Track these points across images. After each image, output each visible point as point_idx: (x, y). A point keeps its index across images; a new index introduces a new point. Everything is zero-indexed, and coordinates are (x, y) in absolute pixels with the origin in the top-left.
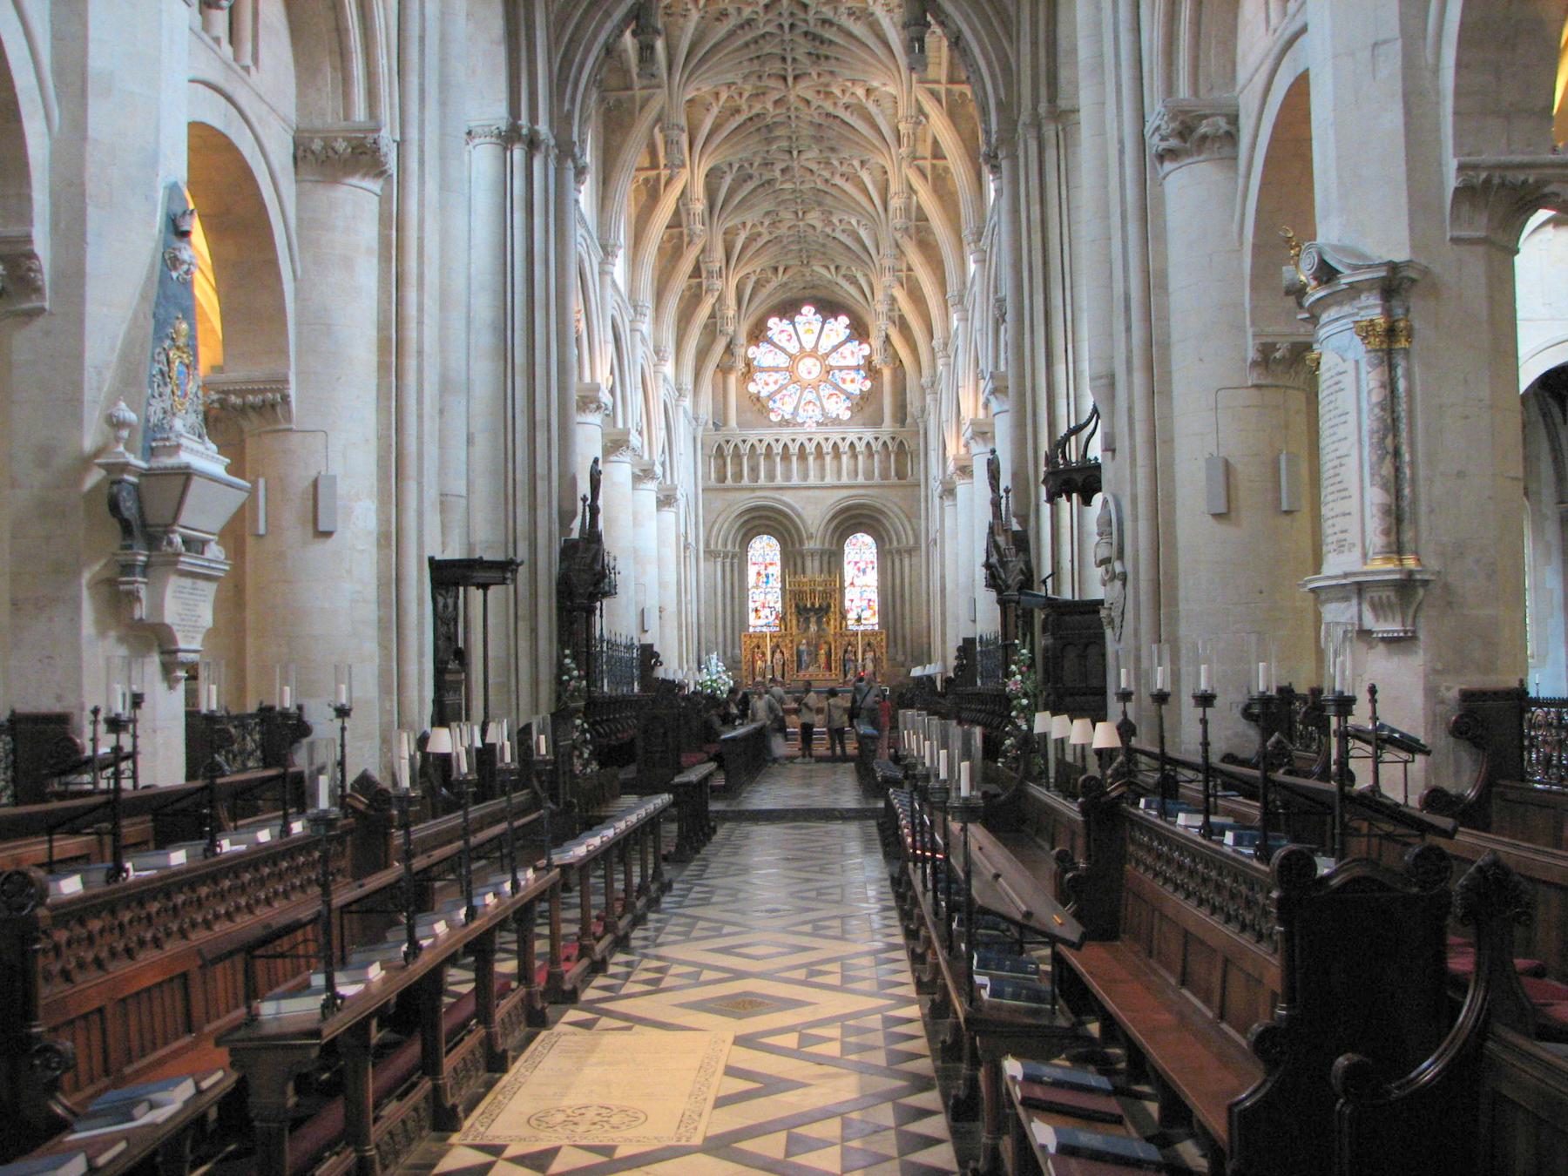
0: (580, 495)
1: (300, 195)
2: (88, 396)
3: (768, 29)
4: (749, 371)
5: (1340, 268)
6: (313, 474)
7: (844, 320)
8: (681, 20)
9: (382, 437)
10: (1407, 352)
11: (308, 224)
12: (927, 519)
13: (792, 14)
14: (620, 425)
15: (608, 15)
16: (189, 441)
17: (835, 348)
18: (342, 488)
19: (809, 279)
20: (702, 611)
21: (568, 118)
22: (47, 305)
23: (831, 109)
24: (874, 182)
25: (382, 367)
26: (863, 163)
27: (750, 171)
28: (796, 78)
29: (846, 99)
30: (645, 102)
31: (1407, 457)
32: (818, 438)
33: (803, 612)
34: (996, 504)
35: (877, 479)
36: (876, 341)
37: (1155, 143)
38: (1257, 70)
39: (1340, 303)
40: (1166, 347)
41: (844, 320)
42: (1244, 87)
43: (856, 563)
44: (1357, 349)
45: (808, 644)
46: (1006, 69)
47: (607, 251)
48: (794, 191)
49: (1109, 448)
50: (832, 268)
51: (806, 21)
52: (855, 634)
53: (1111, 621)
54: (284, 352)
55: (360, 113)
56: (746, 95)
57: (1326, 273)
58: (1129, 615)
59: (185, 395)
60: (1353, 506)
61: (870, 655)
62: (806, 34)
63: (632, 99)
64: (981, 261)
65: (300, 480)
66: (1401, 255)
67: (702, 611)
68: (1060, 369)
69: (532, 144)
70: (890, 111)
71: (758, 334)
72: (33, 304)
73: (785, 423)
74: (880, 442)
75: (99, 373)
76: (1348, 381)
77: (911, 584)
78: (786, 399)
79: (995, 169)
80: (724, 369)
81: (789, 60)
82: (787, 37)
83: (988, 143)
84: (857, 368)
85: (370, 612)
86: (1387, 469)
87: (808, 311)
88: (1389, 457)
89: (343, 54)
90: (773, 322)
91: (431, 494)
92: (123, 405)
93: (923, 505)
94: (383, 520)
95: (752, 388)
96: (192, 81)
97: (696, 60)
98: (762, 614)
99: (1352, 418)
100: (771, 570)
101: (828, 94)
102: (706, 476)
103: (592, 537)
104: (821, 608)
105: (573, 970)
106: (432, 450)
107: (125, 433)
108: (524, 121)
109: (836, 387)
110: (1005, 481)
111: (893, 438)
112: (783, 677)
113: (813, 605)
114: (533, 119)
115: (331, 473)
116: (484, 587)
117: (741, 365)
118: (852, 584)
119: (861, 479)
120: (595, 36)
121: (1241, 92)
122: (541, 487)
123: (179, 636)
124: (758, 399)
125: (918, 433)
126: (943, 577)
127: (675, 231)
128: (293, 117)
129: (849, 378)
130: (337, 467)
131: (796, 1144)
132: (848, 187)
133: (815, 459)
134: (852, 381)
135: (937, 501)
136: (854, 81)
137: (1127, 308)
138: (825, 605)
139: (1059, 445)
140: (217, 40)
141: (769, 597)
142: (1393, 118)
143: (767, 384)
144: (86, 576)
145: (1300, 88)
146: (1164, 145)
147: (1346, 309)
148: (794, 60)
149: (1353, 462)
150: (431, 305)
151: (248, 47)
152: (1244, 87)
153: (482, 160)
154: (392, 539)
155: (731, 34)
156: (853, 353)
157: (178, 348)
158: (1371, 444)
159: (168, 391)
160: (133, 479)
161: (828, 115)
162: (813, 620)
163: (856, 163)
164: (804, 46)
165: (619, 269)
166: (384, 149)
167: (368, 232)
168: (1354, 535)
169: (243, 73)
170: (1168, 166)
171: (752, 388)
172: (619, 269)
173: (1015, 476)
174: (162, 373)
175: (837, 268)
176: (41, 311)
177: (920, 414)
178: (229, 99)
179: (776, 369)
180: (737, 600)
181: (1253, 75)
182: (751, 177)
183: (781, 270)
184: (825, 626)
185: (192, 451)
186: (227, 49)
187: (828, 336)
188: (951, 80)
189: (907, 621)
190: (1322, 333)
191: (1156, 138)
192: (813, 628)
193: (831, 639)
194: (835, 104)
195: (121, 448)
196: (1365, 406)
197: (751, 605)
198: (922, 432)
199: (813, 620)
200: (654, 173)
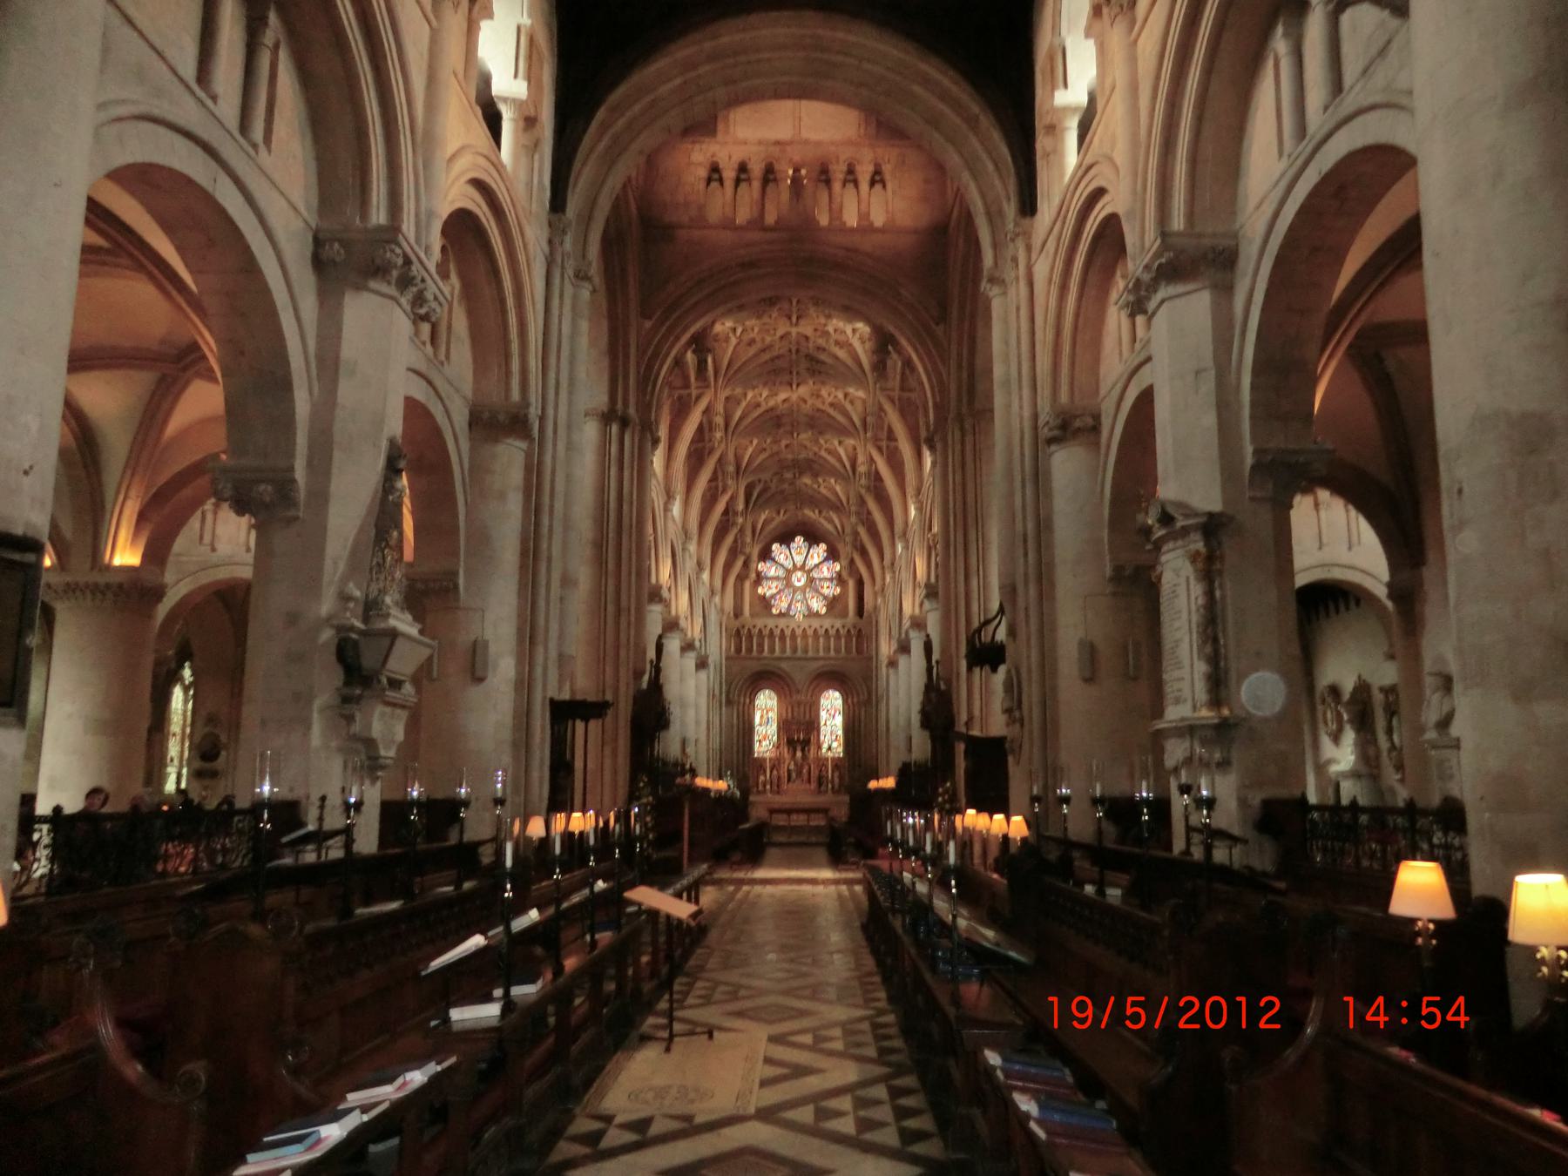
0: (648, 659)
1: (473, 449)
2: (326, 578)
3: (781, 351)
5: (1176, 515)
6: (473, 638)
7: (823, 546)
8: (724, 345)
9: (520, 616)
10: (1220, 573)
11: (478, 471)
13: (798, 343)
14: (673, 612)
15: (678, 338)
16: (394, 611)
17: (817, 566)
18: (493, 649)
19: (800, 518)
21: (649, 406)
22: (301, 515)
23: (821, 407)
24: (848, 456)
25: (523, 567)
26: (840, 443)
27: (765, 446)
28: (798, 385)
29: (830, 399)
30: (698, 398)
31: (1222, 642)
32: (805, 625)
33: (791, 743)
34: (929, 670)
36: (845, 562)
37: (1045, 433)
38: (1112, 388)
39: (1175, 539)
40: (1051, 566)
41: (823, 546)
42: (1105, 397)
44: (1188, 569)
45: (796, 764)
46: (941, 382)
47: (669, 496)
48: (793, 460)
49: (1012, 632)
50: (817, 511)
51: (808, 348)
52: (827, 759)
53: (1013, 751)
54: (456, 554)
55: (516, 395)
56: (764, 395)
57: (1166, 519)
58: (1026, 747)
59: (393, 579)
60: (1185, 672)
61: (836, 774)
62: (807, 356)
63: (690, 395)
64: (920, 509)
65: (464, 639)
66: (1216, 506)
68: (974, 583)
69: (624, 423)
71: (766, 555)
72: (292, 513)
73: (781, 615)
75: (335, 563)
76: (1182, 591)
79: (932, 448)
80: (741, 579)
81: (795, 373)
82: (794, 356)
83: (928, 430)
84: (831, 580)
85: (507, 734)
86: (1208, 649)
87: (799, 540)
88: (1210, 642)
89: (507, 356)
90: (775, 547)
91: (553, 653)
92: (351, 585)
94: (519, 673)
96: (409, 369)
97: (732, 372)
98: (764, 743)
99: (1185, 615)
100: (770, 714)
101: (818, 396)
102: (728, 649)
103: (656, 686)
104: (804, 740)
105: (647, 987)
106: (554, 627)
107: (351, 605)
108: (619, 406)
109: (817, 591)
110: (936, 656)
111: (855, 627)
113: (799, 738)
114: (626, 404)
115: (486, 637)
116: (586, 720)
117: (753, 576)
119: (832, 653)
120: (667, 355)
121: (1102, 400)
122: (623, 653)
123: (381, 746)
125: (871, 622)
126: (888, 722)
127: (713, 484)
128: (469, 394)
129: (826, 585)
130: (489, 634)
131: (823, 1114)
132: (829, 458)
135: (884, 669)
136: (837, 388)
137: (1025, 541)
139: (979, 631)
140: (424, 343)
142: (1210, 419)
144: (317, 704)
145: (1146, 397)
146: (1051, 434)
147: (1180, 543)
148: (798, 373)
149: (1185, 646)
150: (558, 528)
151: (443, 349)
152: (1105, 397)
153: (590, 432)
154: (524, 684)
155: (756, 355)
157: (391, 548)
158: (1198, 632)
159: (382, 577)
160: (354, 636)
161: (818, 410)
162: (799, 748)
163: (836, 443)
164: (804, 364)
165: (676, 509)
166: (531, 421)
167: (516, 476)
168: (1187, 693)
169: (440, 367)
170: (1053, 448)
171: (760, 591)
172: (676, 509)
173: (943, 651)
174: (378, 564)
175: (820, 512)
176: (297, 518)
178: (430, 382)
179: (777, 578)
181: (1110, 391)
182: (765, 450)
184: (806, 752)
185: (397, 618)
186: (429, 348)
187: (812, 557)
188: (902, 389)
190: (1164, 558)
191: (1046, 430)
192: (799, 754)
193: (811, 761)
194: (824, 403)
195: (348, 614)
196: (1193, 608)
197: (756, 738)
198: (874, 623)
199: (799, 748)
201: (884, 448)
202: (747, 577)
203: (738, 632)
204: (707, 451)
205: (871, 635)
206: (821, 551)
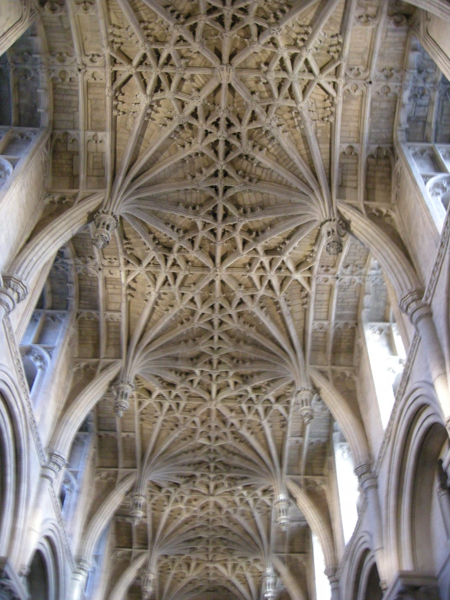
19: (212, 579)
24: (274, 436)
27: (177, 415)
50: (230, 566)
70: (299, 316)
183: (193, 565)
200: (95, 360)
201: (330, 374)
204: (100, 367)
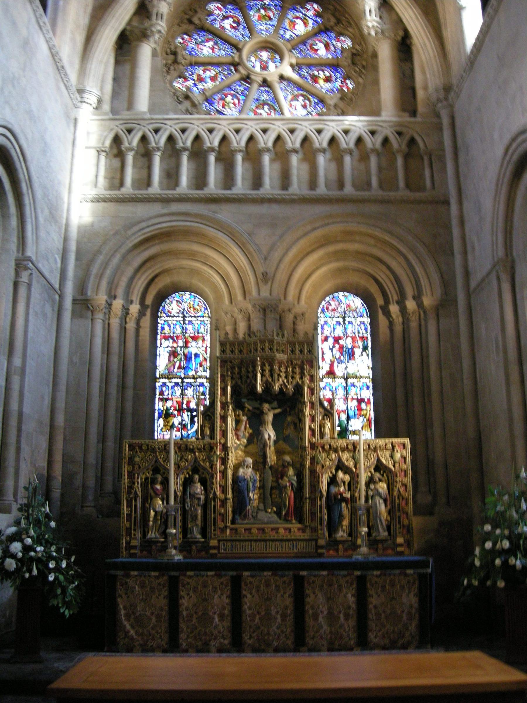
4: (175, 62)
12: (465, 252)
17: (304, 41)
20: (61, 404)
35: (375, 191)
43: (337, 340)
67: (61, 404)
74: (379, 139)
77: (439, 364)
78: (229, 99)
84: (334, 66)
93: (456, 232)
95: (179, 85)
98: (176, 421)
112: (204, 532)
118: (331, 373)
119: (349, 189)
124: (187, 97)
125: (439, 128)
133: (272, 161)
134: (328, 80)
138: (291, 388)
141: (189, 392)
143: (201, 79)
156: (327, 46)
177: (442, 95)
180: (130, 393)
189: (437, 430)
197: (159, 406)
198: (446, 121)
202: (144, 35)
203: (117, 140)
205: (442, 159)
206: (310, 14)
